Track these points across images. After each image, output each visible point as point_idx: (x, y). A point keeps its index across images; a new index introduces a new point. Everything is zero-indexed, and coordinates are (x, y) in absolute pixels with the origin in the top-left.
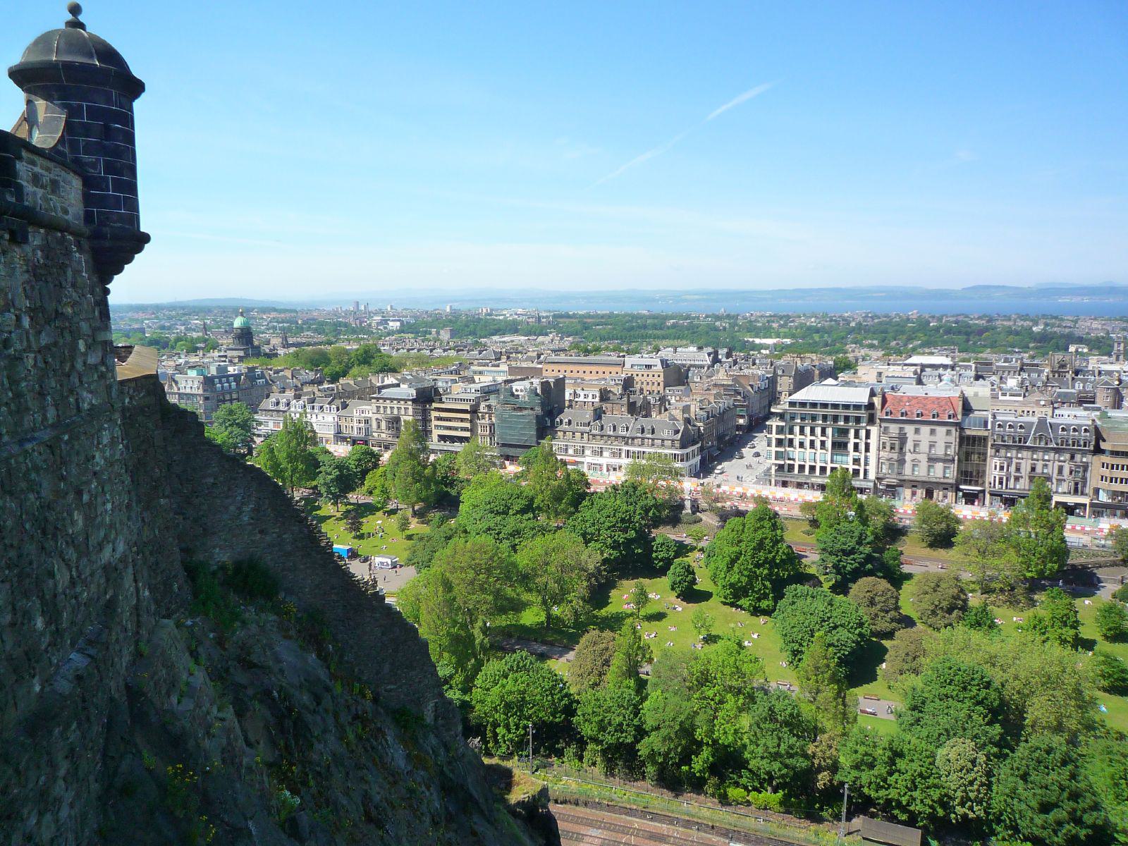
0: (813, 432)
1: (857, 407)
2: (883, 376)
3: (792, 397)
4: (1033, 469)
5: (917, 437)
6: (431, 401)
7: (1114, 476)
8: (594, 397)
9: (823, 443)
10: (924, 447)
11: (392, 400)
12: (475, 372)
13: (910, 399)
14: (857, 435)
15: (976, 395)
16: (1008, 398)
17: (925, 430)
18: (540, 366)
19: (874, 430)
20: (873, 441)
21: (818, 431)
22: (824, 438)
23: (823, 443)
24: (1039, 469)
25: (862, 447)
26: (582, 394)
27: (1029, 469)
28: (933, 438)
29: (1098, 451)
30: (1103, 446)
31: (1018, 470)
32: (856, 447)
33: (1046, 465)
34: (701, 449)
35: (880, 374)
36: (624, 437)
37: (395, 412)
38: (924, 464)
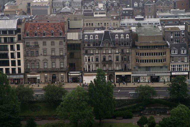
1: (11, 32)
4: (104, 59)
5: (45, 47)
7: (142, 59)
10: (49, 52)
14: (12, 48)
16: (98, 15)
17: (49, 42)
19: (21, 45)
24: (107, 59)
27: (102, 59)
28: (53, 47)
29: (134, 46)
30: (137, 44)
31: (97, 60)
32: (12, 55)
33: (110, 56)
35: (29, 4)
38: (50, 62)
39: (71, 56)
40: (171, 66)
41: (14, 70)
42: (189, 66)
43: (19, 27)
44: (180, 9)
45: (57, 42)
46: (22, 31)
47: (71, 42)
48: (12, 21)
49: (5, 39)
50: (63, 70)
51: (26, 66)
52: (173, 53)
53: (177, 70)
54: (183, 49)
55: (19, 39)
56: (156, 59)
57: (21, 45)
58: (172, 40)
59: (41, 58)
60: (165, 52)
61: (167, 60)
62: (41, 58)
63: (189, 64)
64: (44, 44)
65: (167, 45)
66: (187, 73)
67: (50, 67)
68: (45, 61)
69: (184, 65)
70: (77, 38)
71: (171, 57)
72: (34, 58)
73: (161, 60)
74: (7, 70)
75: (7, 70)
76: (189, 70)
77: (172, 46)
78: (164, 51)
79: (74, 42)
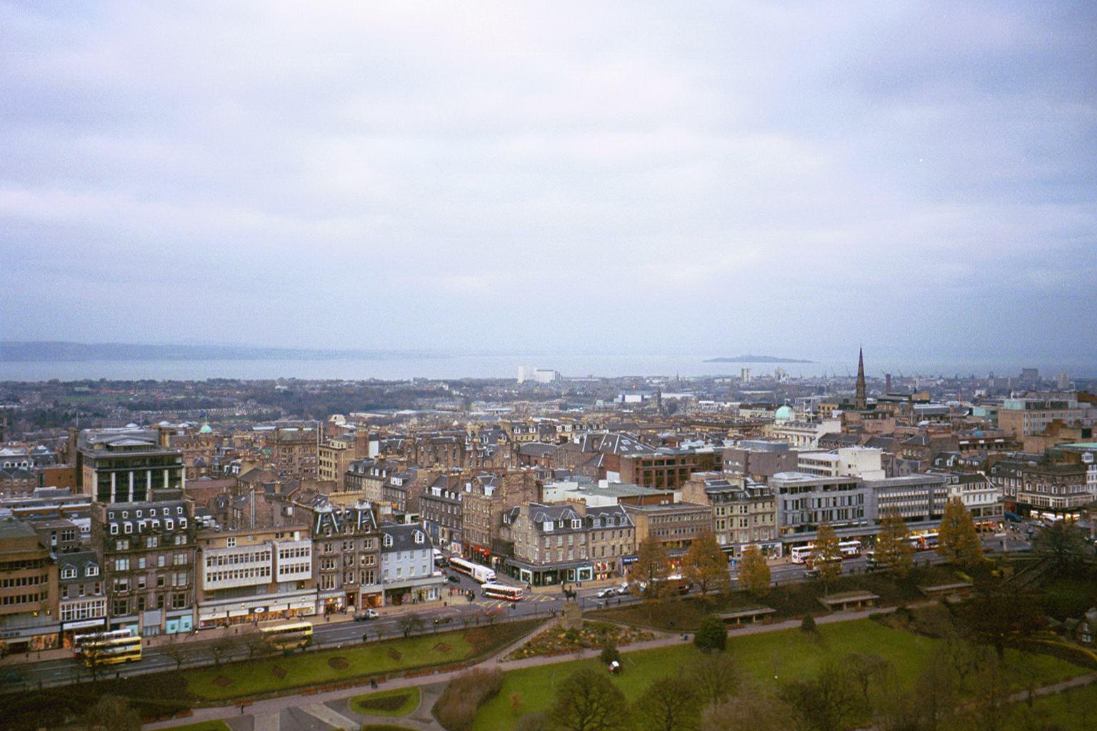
40: (61, 609)
42: (105, 604)
44: (58, 487)
52: (66, 577)
53: (76, 618)
54: (90, 565)
56: (22, 593)
58: (55, 549)
60: (46, 576)
61: (50, 596)
63: (105, 599)
65: (50, 561)
66: (101, 622)
69: (93, 603)
71: (60, 586)
73: (36, 596)
76: (105, 614)
77: (60, 559)
78: (44, 574)
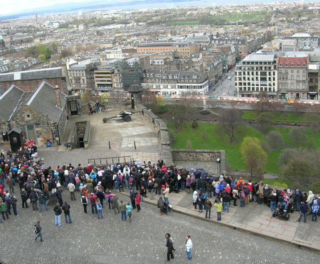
0: (253, 74)
1: (269, 63)
2: (282, 44)
3: (244, 60)
6: (93, 70)
8: (162, 62)
9: (257, 78)
10: (295, 77)
11: (76, 71)
12: (107, 53)
13: (289, 58)
14: (270, 74)
15: (315, 55)
17: (295, 71)
18: (135, 48)
19: (276, 72)
20: (276, 76)
21: (255, 73)
22: (257, 76)
23: (257, 78)
25: (272, 79)
26: (156, 61)
32: (270, 78)
34: (209, 82)
36: (176, 80)
37: (78, 75)
38: (295, 84)
39: (311, 81)
41: (270, 89)
43: (276, 59)
45: (301, 71)
46: (277, 62)
47: (311, 71)
48: (271, 55)
49: (265, 68)
50: (305, 90)
51: (278, 87)
55: (275, 68)
57: (276, 72)
59: (289, 82)
62: (289, 82)
64: (292, 72)
67: (295, 88)
68: (292, 84)
70: (316, 69)
72: (284, 82)
74: (266, 89)
75: (266, 89)
79: (313, 71)
